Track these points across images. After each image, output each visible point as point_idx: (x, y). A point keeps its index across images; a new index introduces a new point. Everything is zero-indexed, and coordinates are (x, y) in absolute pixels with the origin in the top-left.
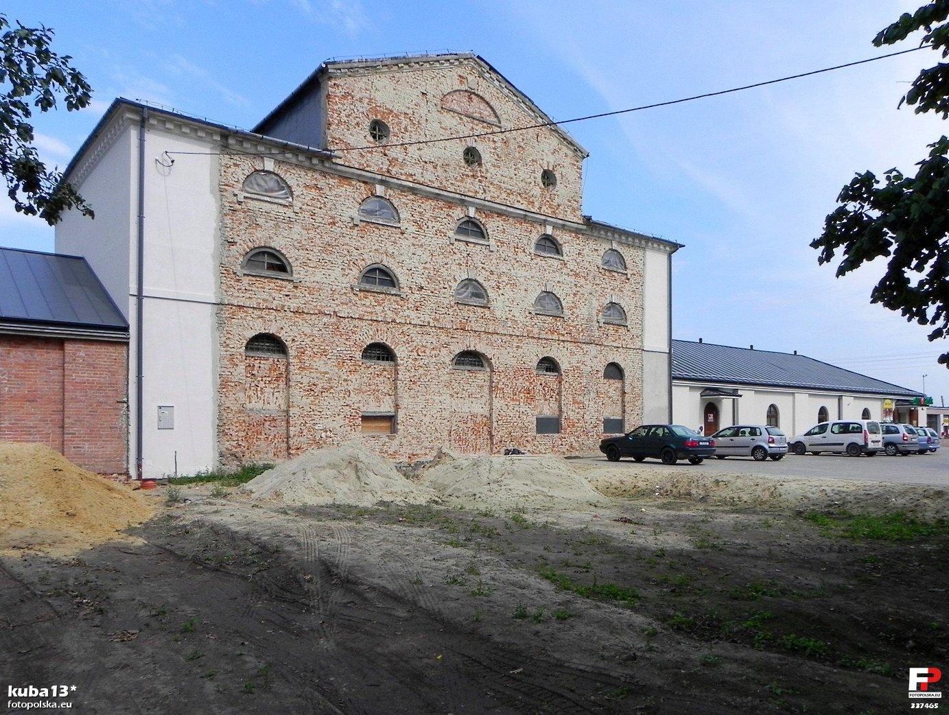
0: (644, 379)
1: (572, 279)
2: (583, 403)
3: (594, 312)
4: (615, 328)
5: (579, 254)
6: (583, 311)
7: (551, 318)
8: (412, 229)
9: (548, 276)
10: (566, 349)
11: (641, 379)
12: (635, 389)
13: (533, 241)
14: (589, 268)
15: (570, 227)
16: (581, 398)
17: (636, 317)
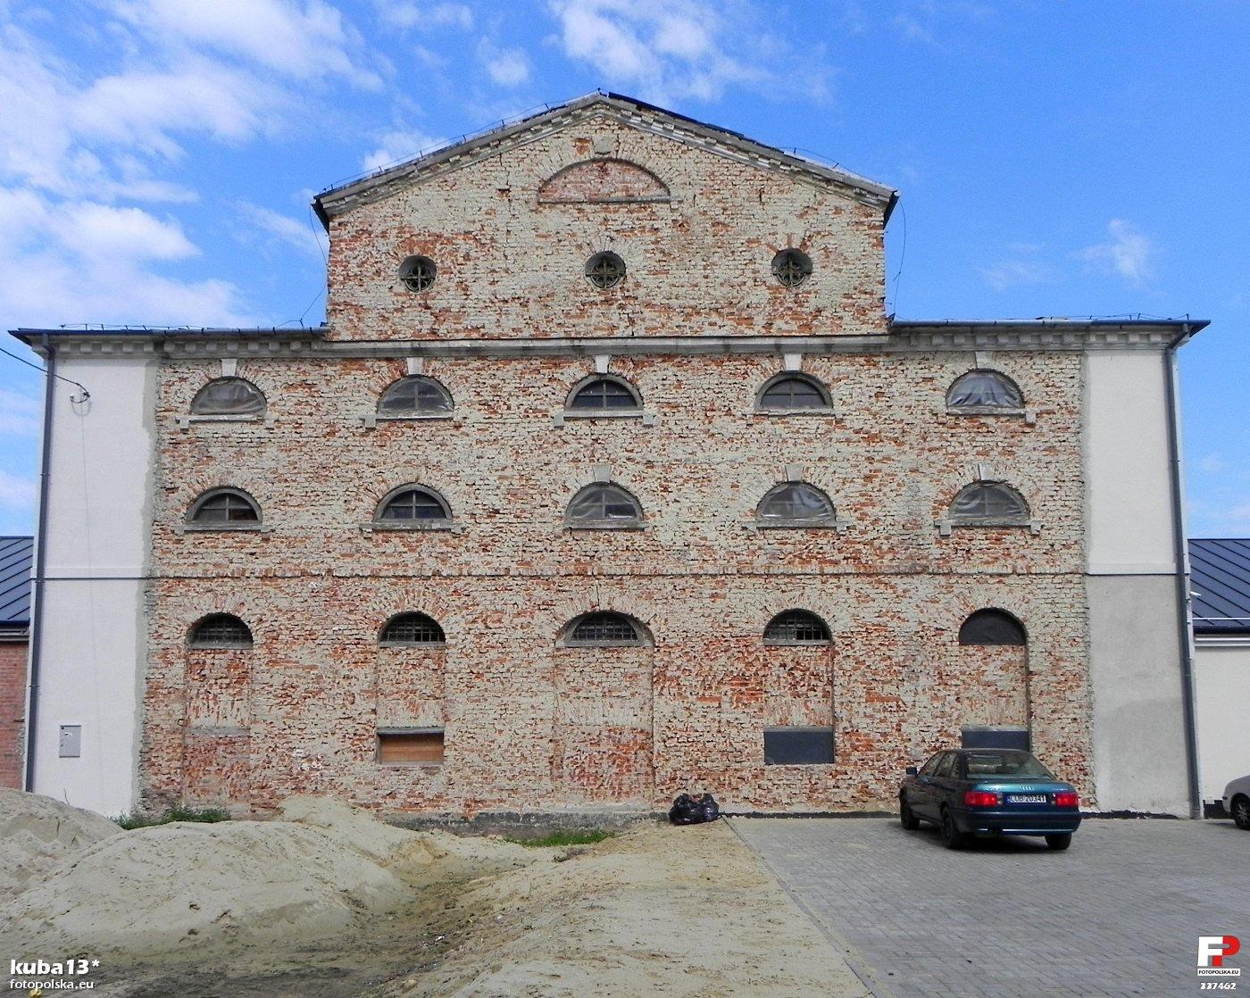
4: (994, 534)
6: (895, 508)
12: (1062, 664)
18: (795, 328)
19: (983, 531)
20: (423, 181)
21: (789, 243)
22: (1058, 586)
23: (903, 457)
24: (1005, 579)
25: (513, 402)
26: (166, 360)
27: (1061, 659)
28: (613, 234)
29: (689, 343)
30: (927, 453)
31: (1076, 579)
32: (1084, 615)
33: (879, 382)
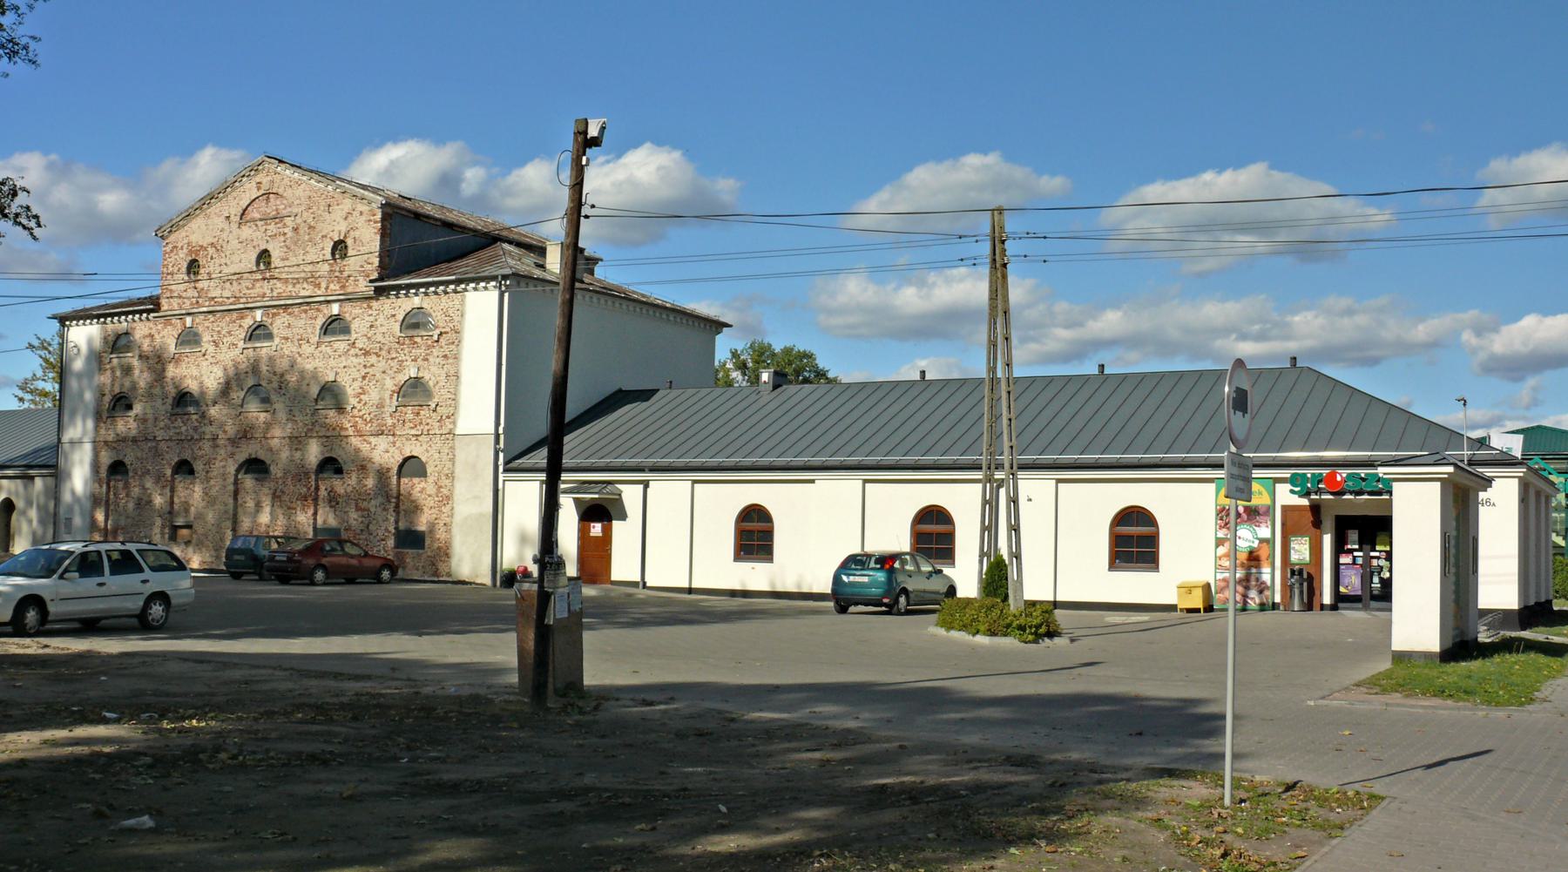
0: (456, 474)
1: (361, 360)
2: (368, 510)
3: (387, 396)
5: (372, 326)
6: (373, 396)
8: (211, 349)
11: (451, 476)
12: (442, 490)
14: (383, 341)
16: (365, 503)
17: (447, 390)
18: (338, 288)
20: (197, 216)
21: (339, 236)
23: (379, 364)
24: (420, 438)
25: (225, 341)
27: (441, 487)
28: (268, 238)
30: (390, 361)
32: (452, 460)
33: (372, 318)
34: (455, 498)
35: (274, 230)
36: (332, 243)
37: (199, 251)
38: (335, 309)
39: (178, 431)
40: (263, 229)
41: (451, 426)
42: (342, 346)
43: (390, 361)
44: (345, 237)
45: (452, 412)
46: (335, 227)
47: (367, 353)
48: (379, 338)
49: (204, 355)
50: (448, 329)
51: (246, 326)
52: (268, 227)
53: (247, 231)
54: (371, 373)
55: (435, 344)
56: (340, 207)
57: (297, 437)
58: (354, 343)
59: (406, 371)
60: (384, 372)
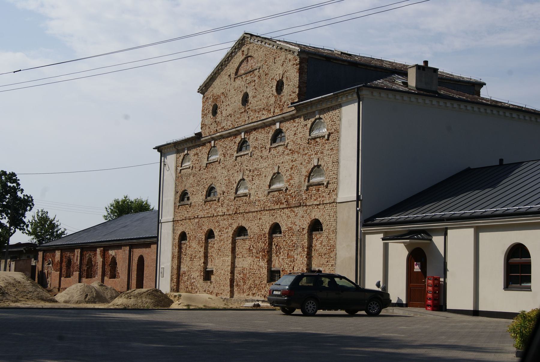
3: (303, 179)
4: (317, 187)
5: (295, 134)
7: (277, 192)
9: (276, 160)
10: (284, 214)
11: (335, 232)
12: (331, 241)
13: (270, 138)
15: (287, 117)
18: (279, 111)
19: (315, 187)
21: (279, 78)
22: (331, 208)
24: (319, 207)
25: (228, 153)
26: (178, 152)
28: (247, 85)
29: (255, 124)
30: (304, 156)
31: (334, 204)
32: (335, 220)
34: (337, 247)
35: (250, 80)
36: (276, 82)
37: (217, 98)
38: (278, 126)
39: (208, 211)
40: (244, 79)
41: (335, 197)
42: (281, 149)
43: (304, 156)
44: (282, 77)
45: (335, 187)
46: (277, 72)
47: (293, 152)
48: (299, 141)
49: (219, 163)
50: (333, 130)
51: (237, 142)
52: (247, 78)
53: (238, 82)
54: (295, 165)
55: (327, 142)
56: (280, 58)
57: (260, 211)
58: (287, 146)
59: (312, 162)
60: (301, 164)
